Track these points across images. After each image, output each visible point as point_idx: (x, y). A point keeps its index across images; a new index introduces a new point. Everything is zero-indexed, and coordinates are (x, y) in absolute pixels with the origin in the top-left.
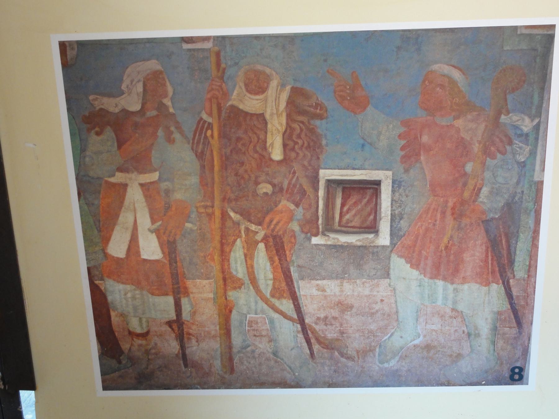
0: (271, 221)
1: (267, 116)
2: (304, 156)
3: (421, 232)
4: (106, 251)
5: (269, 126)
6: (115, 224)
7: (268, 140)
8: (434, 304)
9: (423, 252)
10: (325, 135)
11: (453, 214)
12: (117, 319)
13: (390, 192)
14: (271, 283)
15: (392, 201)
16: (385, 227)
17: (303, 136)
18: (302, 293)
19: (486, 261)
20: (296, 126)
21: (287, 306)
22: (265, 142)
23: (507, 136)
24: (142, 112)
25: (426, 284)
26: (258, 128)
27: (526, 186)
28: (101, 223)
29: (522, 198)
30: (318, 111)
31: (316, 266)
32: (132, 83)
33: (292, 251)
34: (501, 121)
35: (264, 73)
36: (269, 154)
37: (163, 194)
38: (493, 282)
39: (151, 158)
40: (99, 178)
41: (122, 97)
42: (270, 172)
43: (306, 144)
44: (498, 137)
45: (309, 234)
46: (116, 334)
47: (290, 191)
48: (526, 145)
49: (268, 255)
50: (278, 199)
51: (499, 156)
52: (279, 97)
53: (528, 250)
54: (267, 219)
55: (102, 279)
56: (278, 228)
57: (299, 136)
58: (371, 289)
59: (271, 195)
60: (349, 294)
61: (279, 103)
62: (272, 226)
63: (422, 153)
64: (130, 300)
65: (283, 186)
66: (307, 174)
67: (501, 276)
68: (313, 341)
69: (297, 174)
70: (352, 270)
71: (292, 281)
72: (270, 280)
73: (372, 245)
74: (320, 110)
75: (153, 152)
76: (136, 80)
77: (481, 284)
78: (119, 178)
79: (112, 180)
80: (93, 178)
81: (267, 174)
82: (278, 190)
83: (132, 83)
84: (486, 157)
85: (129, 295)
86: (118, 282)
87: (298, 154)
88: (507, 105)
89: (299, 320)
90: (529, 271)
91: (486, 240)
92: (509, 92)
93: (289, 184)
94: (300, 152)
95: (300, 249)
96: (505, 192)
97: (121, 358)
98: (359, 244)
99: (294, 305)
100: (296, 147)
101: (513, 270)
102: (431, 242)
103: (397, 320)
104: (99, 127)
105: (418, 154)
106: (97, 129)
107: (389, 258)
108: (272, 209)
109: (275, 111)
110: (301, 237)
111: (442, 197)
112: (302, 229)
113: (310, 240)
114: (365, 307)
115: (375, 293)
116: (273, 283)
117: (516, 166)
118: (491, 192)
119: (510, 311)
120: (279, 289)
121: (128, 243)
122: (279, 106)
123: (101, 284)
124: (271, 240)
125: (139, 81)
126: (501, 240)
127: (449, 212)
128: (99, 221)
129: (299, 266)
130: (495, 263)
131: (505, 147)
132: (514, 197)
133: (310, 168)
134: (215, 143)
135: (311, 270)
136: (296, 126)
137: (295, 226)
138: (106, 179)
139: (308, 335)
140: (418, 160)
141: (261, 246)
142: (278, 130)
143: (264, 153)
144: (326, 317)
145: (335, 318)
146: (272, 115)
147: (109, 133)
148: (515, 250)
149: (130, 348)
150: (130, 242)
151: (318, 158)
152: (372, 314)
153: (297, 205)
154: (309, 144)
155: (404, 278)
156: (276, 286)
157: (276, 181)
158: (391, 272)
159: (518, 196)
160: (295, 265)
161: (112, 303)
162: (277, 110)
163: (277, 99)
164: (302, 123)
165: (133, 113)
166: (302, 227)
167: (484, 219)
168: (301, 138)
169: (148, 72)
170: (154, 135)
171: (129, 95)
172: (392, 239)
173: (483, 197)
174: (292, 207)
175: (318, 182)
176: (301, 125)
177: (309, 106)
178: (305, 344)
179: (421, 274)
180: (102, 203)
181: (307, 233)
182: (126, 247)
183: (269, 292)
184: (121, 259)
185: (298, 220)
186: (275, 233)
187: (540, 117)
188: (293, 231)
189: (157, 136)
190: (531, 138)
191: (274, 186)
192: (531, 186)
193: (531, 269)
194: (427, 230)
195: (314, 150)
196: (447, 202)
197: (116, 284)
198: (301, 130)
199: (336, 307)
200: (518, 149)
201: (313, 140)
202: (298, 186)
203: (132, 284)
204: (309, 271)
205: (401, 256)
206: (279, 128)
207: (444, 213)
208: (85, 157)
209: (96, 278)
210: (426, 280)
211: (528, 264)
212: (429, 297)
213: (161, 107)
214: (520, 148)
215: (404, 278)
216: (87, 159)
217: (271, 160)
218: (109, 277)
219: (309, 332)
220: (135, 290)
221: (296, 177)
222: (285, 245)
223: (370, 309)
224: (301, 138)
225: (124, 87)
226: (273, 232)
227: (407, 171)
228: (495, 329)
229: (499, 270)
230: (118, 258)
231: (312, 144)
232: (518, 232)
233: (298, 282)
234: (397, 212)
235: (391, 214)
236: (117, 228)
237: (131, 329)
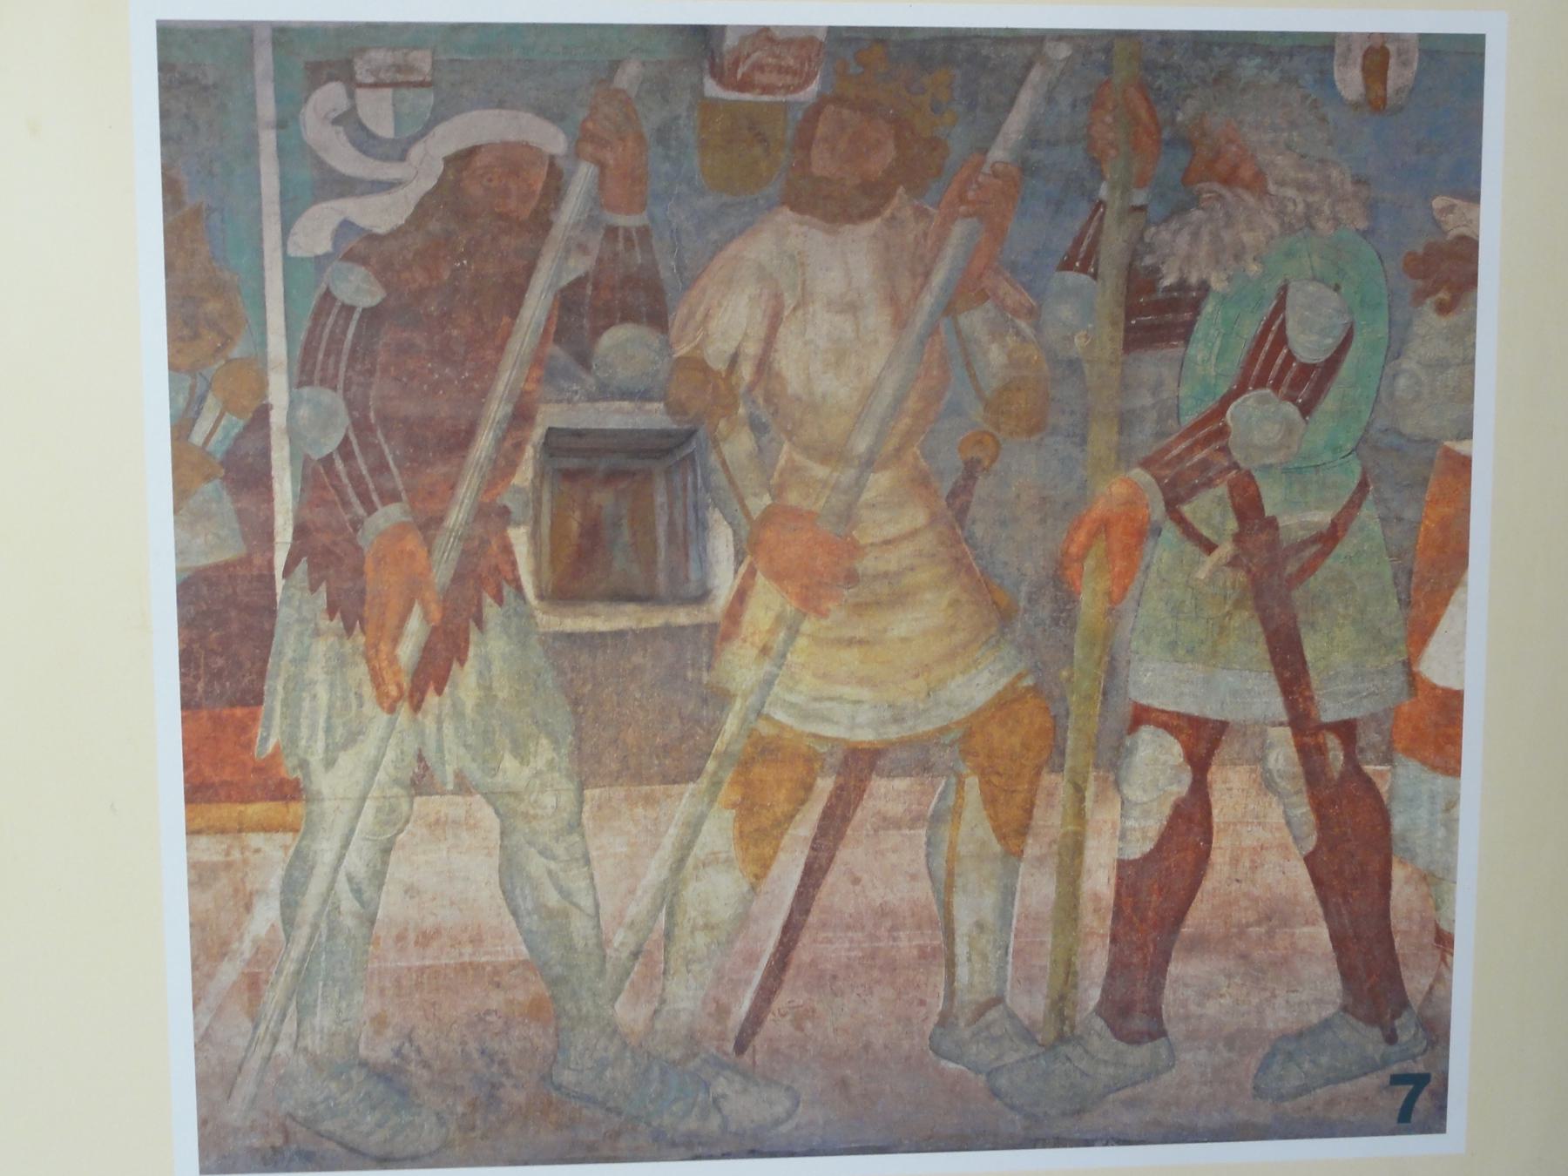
55: (1387, 759)
86: (1434, 768)
97: (1397, 1023)
123: (1382, 774)
149: (1431, 988)
161: (1404, 840)
197: (1427, 775)
209: (1370, 755)
218: (1409, 752)
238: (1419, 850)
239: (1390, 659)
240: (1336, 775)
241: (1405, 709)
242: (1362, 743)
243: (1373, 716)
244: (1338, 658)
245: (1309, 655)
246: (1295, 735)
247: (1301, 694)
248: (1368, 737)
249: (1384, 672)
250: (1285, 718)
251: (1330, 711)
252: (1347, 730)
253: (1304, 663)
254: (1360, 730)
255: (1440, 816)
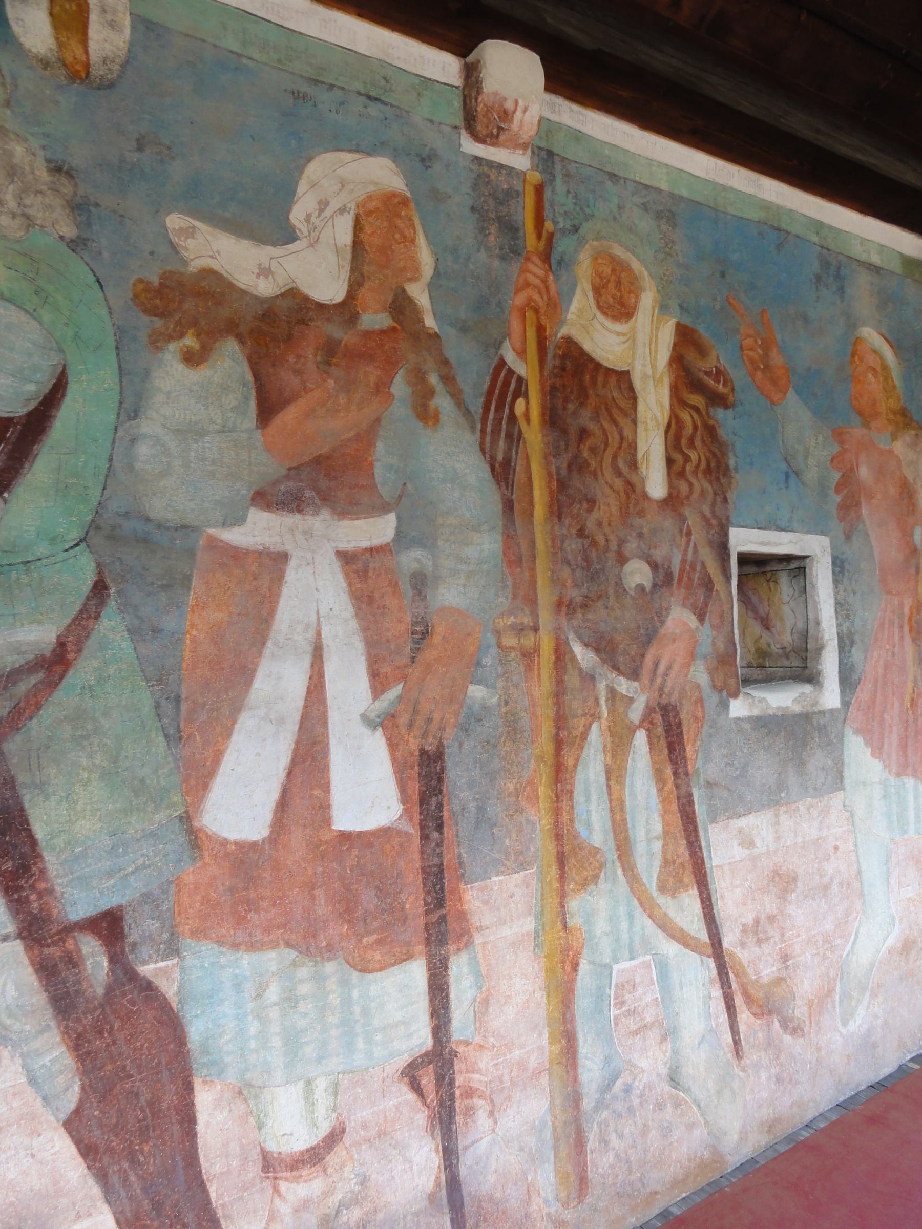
0: (657, 664)
1: (637, 383)
2: (703, 493)
3: (880, 670)
4: (196, 824)
5: (641, 407)
6: (236, 709)
7: (639, 445)
8: (906, 836)
9: (885, 716)
10: (733, 445)
11: (911, 631)
12: (221, 1116)
13: (831, 585)
14: (658, 846)
15: (836, 604)
16: (829, 664)
17: (698, 442)
18: (716, 861)
20: (685, 416)
21: (686, 910)
22: (633, 446)
24: (347, 311)
25: (893, 790)
26: (620, 409)
28: (184, 707)
30: (721, 386)
31: (736, 778)
32: (321, 211)
33: (698, 743)
35: (629, 269)
36: (643, 481)
37: (405, 587)
39: (371, 465)
40: (185, 528)
41: (291, 247)
42: (645, 530)
43: (703, 465)
45: (725, 693)
46: (213, 1191)
47: (685, 579)
49: (654, 763)
50: (665, 605)
52: (657, 336)
54: (649, 660)
55: (172, 950)
56: (669, 683)
57: (691, 444)
58: (821, 822)
59: (652, 592)
60: (788, 843)
61: (656, 352)
62: (659, 680)
63: (862, 500)
64: (274, 1014)
65: (673, 569)
66: (710, 536)
68: (739, 1001)
69: (693, 537)
70: (792, 778)
71: (696, 830)
72: (657, 838)
73: (816, 709)
74: (724, 385)
75: (380, 446)
76: (334, 205)
78: (259, 530)
79: (234, 536)
80: (159, 526)
81: (640, 535)
82: (664, 578)
83: (321, 211)
85: (273, 993)
86: (235, 946)
87: (691, 485)
89: (713, 945)
93: (684, 561)
94: (694, 481)
95: (710, 736)
98: (797, 709)
99: (702, 902)
100: (689, 468)
102: (893, 694)
103: (861, 894)
104: (198, 335)
105: (858, 505)
106: (190, 341)
107: (841, 740)
108: (656, 631)
109: (650, 372)
110: (712, 699)
111: (895, 595)
112: (713, 681)
113: (725, 706)
114: (813, 873)
115: (825, 833)
116: (663, 847)
120: (674, 861)
121: (282, 775)
122: (656, 359)
123: (165, 972)
124: (658, 718)
125: (342, 210)
127: (906, 629)
128: (178, 699)
129: (709, 785)
133: (714, 522)
134: (534, 436)
135: (729, 790)
136: (685, 416)
137: (700, 675)
138: (211, 531)
139: (730, 987)
140: (859, 517)
141: (641, 737)
142: (657, 421)
143: (634, 479)
144: (757, 921)
145: (771, 919)
146: (645, 377)
147: (230, 362)
150: (289, 774)
151: (725, 500)
152: (826, 888)
153: (701, 618)
154: (708, 464)
155: (864, 784)
156: (669, 857)
157: (658, 555)
158: (846, 774)
160: (702, 781)
161: (206, 1051)
162: (654, 367)
163: (653, 340)
164: (697, 409)
165: (321, 306)
166: (712, 672)
168: (695, 448)
169: (371, 189)
170: (381, 389)
171: (311, 245)
172: (843, 692)
174: (693, 622)
175: (729, 556)
176: (695, 416)
177: (706, 373)
178: (724, 1018)
179: (885, 766)
180: (193, 626)
181: (721, 691)
182: (275, 795)
183: (655, 876)
184: (254, 845)
185: (705, 657)
186: (665, 700)
188: (698, 686)
189: (390, 397)
191: (654, 566)
194: (886, 667)
195: (718, 479)
196: (901, 605)
197: (227, 957)
198: (695, 428)
199: (771, 888)
201: (714, 455)
202: (698, 569)
203: (288, 945)
204: (725, 794)
205: (858, 731)
206: (659, 415)
207: (901, 627)
208: (133, 441)
209: (145, 951)
210: (892, 780)
212: (898, 821)
213: (401, 306)
215: (864, 784)
216: (143, 450)
217: (645, 496)
218: (199, 933)
219: (731, 975)
220: (294, 964)
221: (692, 545)
222: (685, 729)
223: (821, 877)
224: (695, 448)
225: (297, 215)
226: (661, 696)
227: (848, 537)
230: (240, 845)
231: (713, 465)
233: (706, 830)
234: (845, 629)
235: (838, 634)
236: (246, 722)
237: (272, 1147)
238: (227, 1059)
239: (161, 817)
240: (100, 991)
241: (189, 879)
242: (133, 936)
243: (146, 897)
244: (85, 827)
245: (40, 831)
246: (28, 949)
247: (32, 887)
248: (137, 929)
249: (153, 835)
250: (11, 928)
251: (78, 901)
252: (109, 926)
253: (34, 843)
254: (128, 920)
255: (250, 1006)
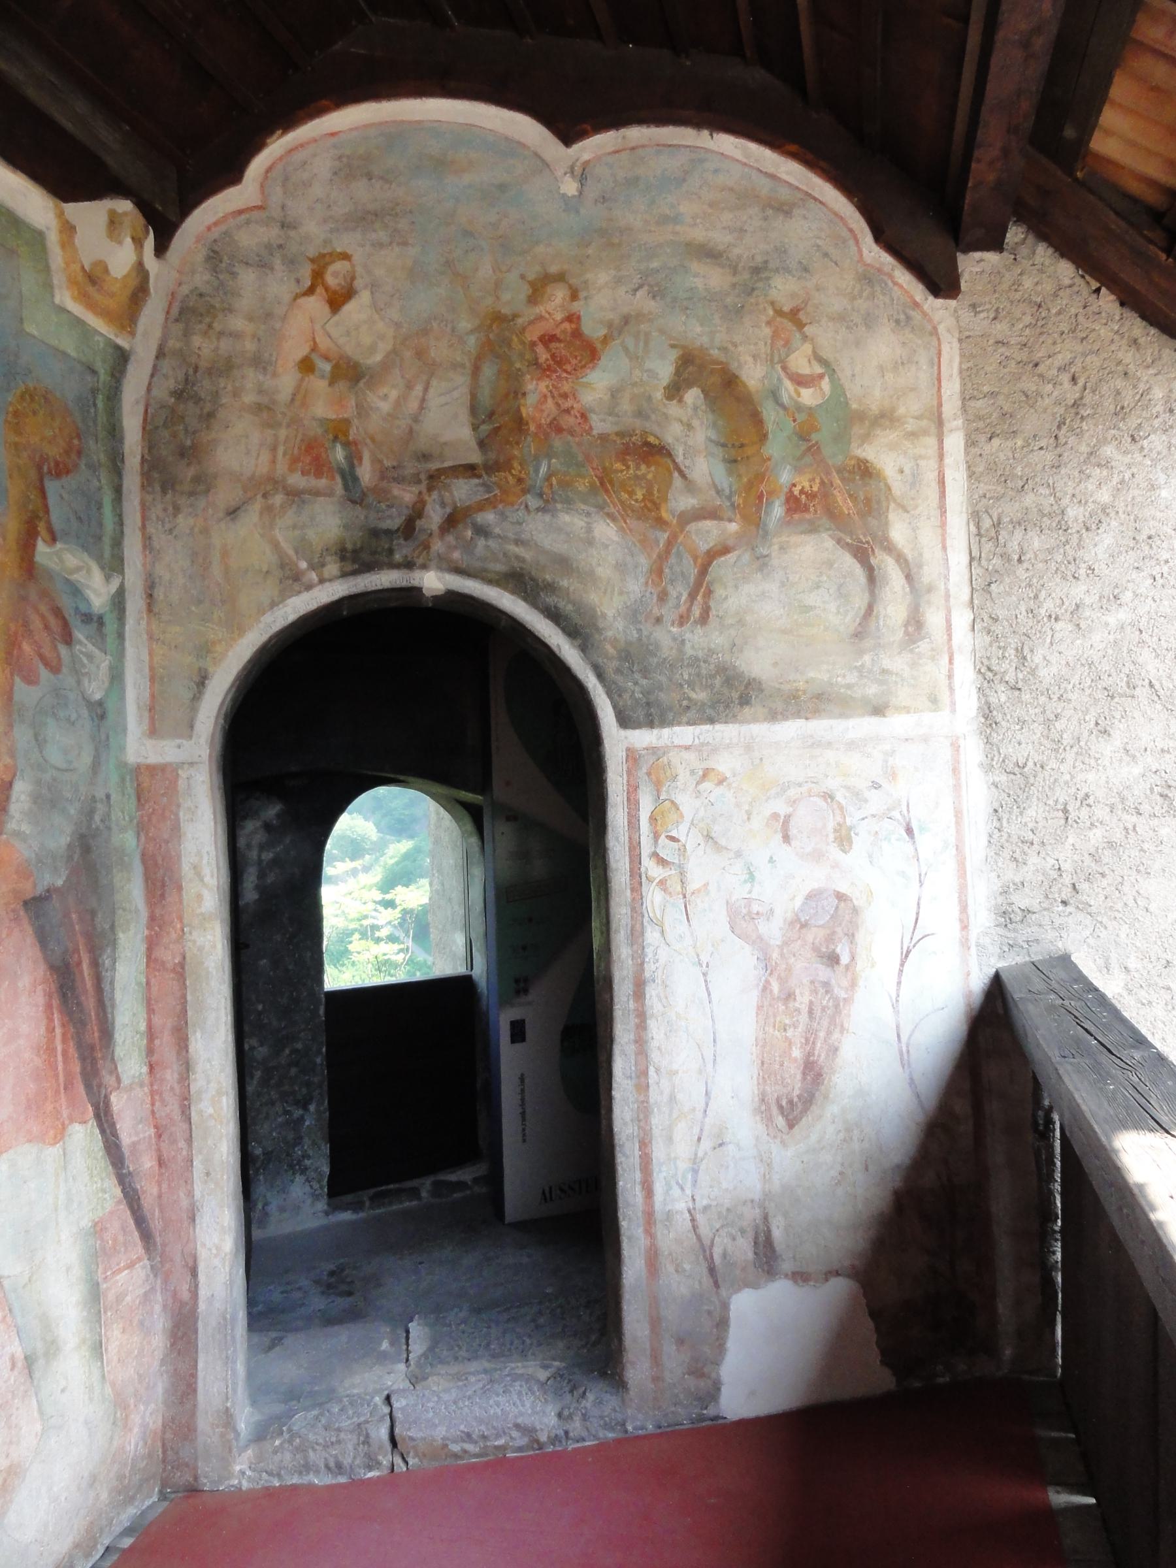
19: (50, 1050)
23: (58, 612)
27: (114, 778)
29: (108, 814)
34: (38, 558)
38: (72, 1120)
44: (37, 610)
48: (100, 649)
51: (44, 673)
53: (139, 984)
67: (88, 1086)
77: (41, 1139)
84: (12, 675)
88: (47, 512)
90: (150, 1051)
91: (42, 970)
92: (50, 472)
96: (69, 795)
101: (113, 1059)
117: (85, 713)
118: (36, 798)
119: (123, 1207)
126: (79, 964)
130: (72, 1051)
131: (55, 647)
132: (91, 813)
148: (113, 990)
159: (101, 808)
167: (28, 896)
173: (17, 815)
187: (122, 572)
190: (111, 627)
192: (123, 780)
193: (157, 1042)
200: (85, 661)
211: (143, 1027)
214: (90, 657)
228: (95, 1296)
229: (83, 1069)
232: (113, 927)
